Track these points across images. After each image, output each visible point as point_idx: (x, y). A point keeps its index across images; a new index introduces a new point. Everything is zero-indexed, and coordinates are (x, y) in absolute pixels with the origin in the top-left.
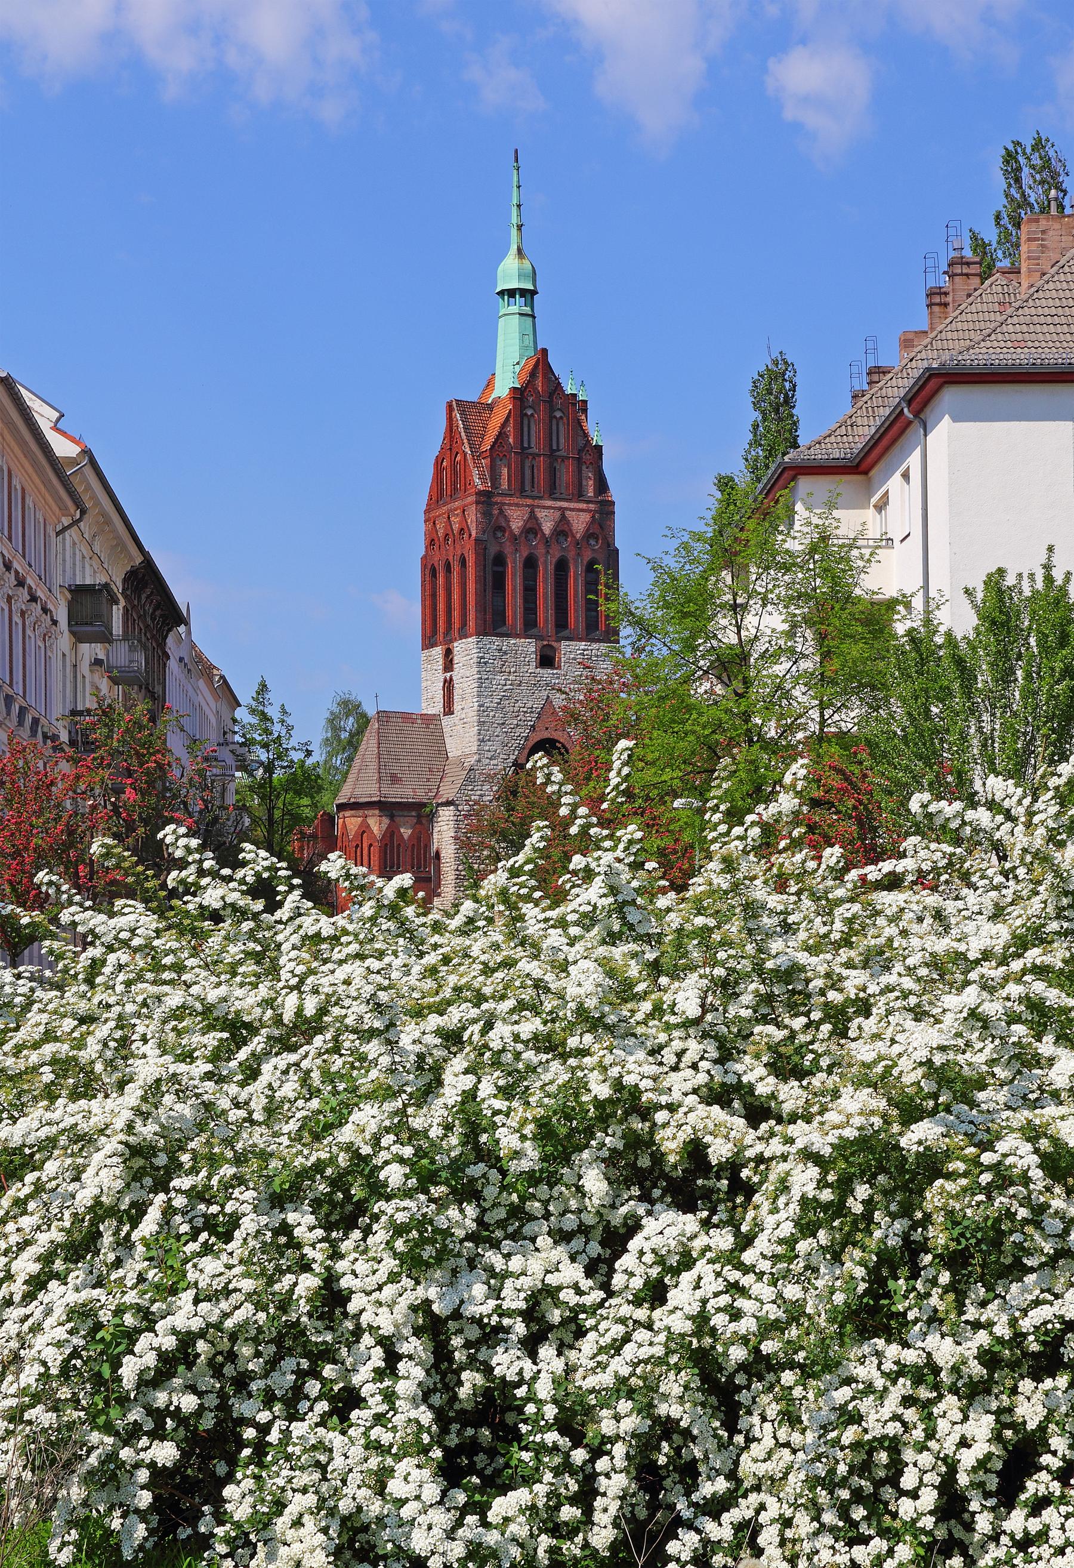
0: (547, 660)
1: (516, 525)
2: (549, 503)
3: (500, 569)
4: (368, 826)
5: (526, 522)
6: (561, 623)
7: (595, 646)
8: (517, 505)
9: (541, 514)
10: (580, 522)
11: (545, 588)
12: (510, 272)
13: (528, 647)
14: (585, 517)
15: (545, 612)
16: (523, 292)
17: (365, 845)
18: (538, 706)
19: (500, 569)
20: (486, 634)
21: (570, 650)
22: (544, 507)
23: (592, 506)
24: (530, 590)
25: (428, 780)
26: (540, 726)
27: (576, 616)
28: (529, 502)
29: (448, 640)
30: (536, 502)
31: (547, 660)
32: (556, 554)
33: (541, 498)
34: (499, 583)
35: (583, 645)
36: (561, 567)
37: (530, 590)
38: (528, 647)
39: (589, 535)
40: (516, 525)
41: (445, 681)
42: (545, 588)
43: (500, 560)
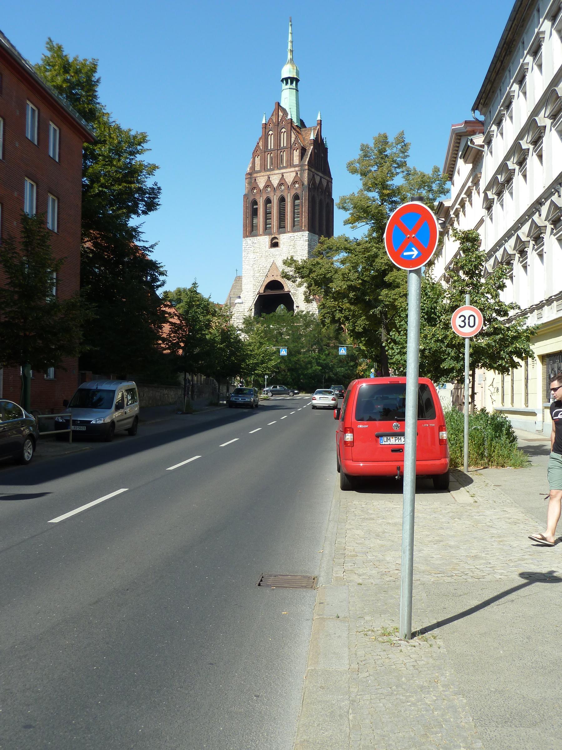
0: (275, 245)
1: (261, 185)
7: (296, 234)
8: (263, 176)
12: (287, 71)
13: (265, 240)
16: (292, 79)
20: (247, 237)
23: (297, 169)
24: (267, 214)
26: (269, 274)
32: (279, 194)
33: (273, 170)
34: (255, 213)
36: (282, 200)
37: (267, 214)
38: (265, 240)
39: (294, 182)
43: (255, 203)
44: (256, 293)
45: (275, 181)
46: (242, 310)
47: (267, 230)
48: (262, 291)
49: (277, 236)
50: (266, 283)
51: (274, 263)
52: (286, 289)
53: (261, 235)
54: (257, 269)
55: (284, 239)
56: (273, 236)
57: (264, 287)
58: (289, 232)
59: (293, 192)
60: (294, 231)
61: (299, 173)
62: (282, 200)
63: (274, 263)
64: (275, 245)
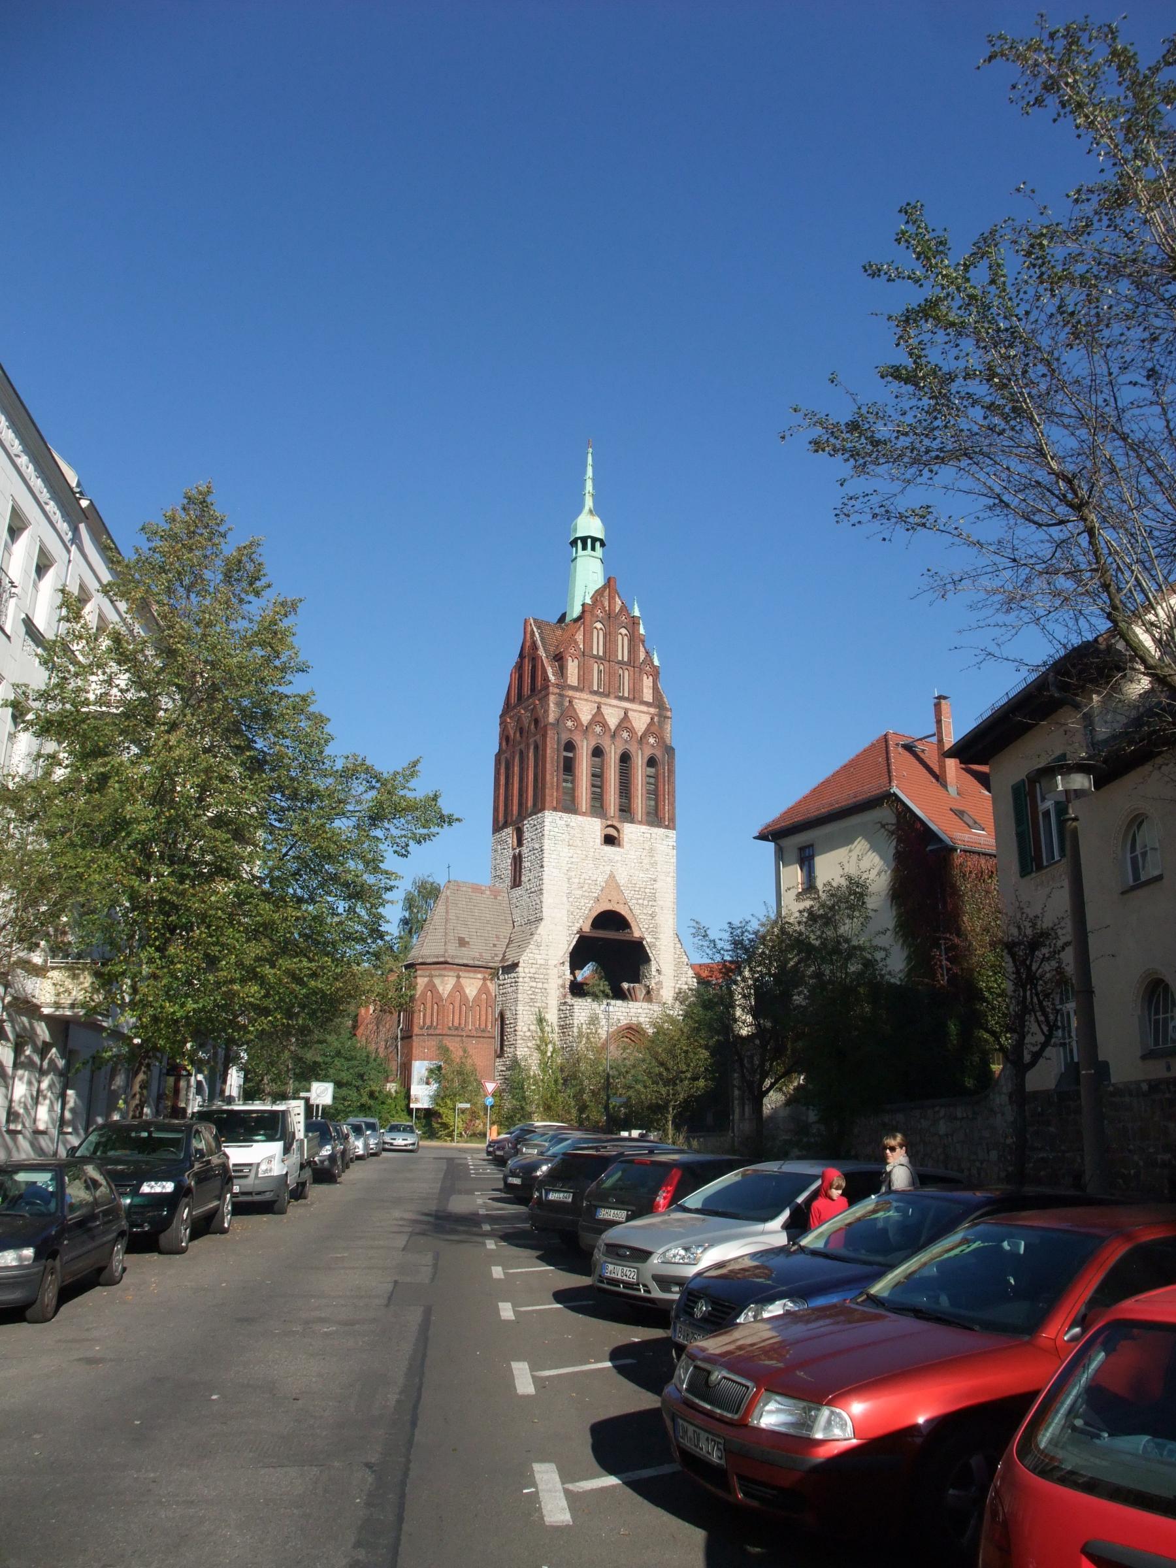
2: (615, 702)
3: (570, 755)
4: (434, 986)
5: (594, 716)
6: (626, 811)
9: (606, 710)
10: (641, 720)
13: (594, 827)
14: (647, 719)
18: (601, 880)
19: (570, 755)
21: (631, 832)
25: (495, 945)
27: (639, 803)
28: (597, 699)
30: (604, 700)
36: (625, 758)
37: (598, 777)
38: (594, 827)
40: (585, 716)
41: (514, 857)
44: (575, 929)
45: (612, 718)
46: (542, 962)
47: (598, 807)
48: (587, 928)
51: (612, 877)
52: (637, 934)
53: (584, 814)
54: (577, 880)
55: (631, 832)
56: (609, 823)
58: (640, 823)
59: (648, 752)
60: (651, 824)
61: (656, 719)
62: (625, 758)
63: (612, 877)
64: (610, 840)
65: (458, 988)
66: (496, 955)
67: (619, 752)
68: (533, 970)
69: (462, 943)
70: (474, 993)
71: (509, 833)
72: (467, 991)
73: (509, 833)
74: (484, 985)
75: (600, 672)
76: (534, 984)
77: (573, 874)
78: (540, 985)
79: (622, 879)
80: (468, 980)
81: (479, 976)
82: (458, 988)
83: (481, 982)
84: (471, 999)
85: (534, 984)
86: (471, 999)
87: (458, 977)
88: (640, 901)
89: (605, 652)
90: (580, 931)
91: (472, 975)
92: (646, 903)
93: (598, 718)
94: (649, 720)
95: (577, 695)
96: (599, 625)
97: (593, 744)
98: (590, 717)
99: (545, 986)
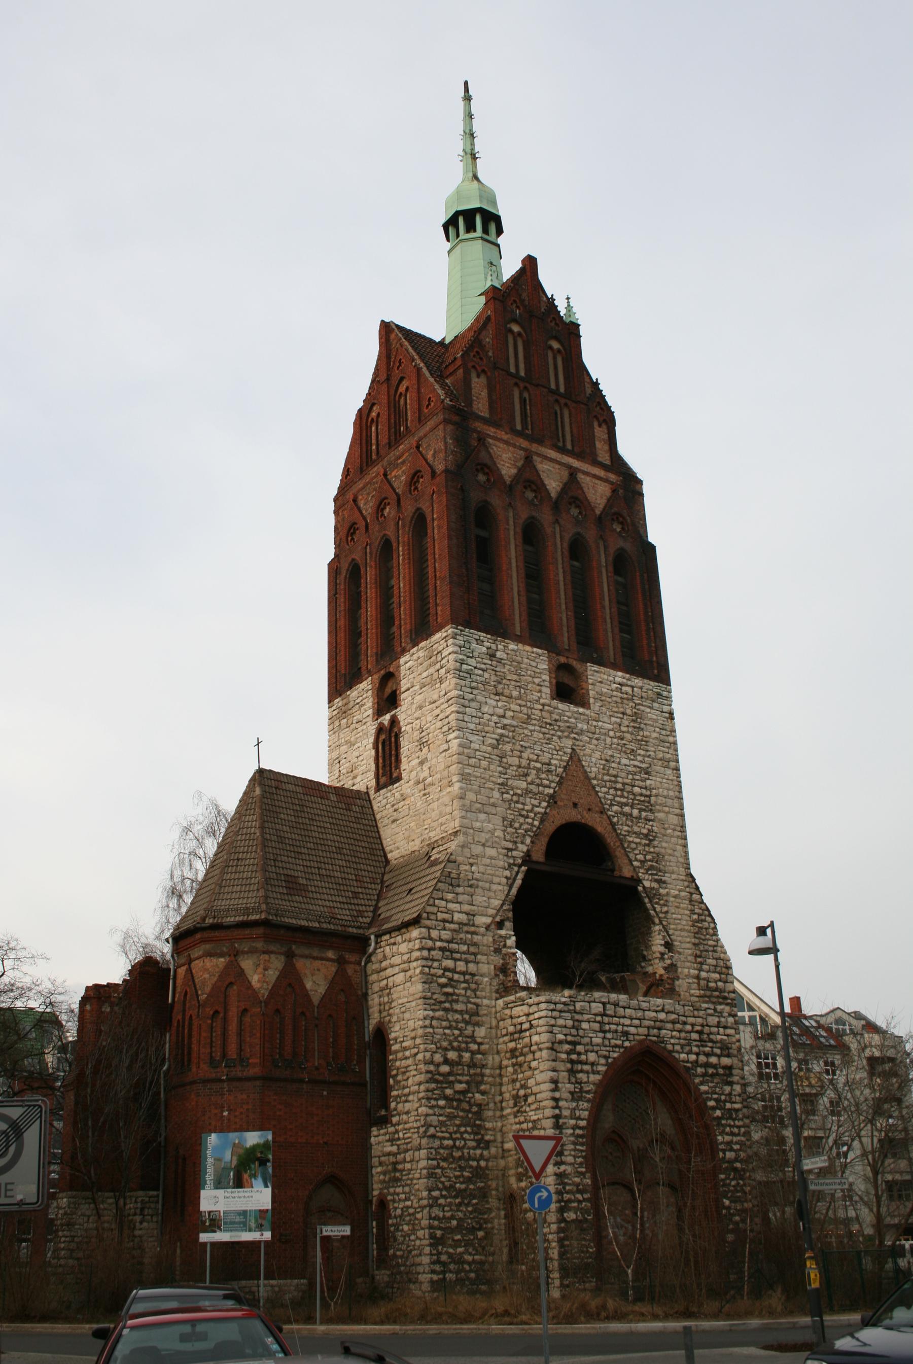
0: (567, 690)
2: (553, 454)
3: (483, 534)
7: (638, 682)
11: (558, 573)
13: (536, 664)
15: (562, 615)
17: (233, 1012)
18: (558, 762)
20: (468, 624)
22: (546, 458)
25: (356, 895)
27: (608, 632)
29: (390, 650)
30: (534, 447)
31: (567, 690)
35: (619, 676)
37: (534, 575)
41: (380, 730)
42: (558, 573)
46: (463, 918)
49: (574, 663)
50: (550, 828)
51: (574, 757)
52: (627, 872)
54: (515, 761)
56: (563, 660)
57: (543, 842)
63: (574, 757)
65: (290, 980)
66: (361, 914)
67: (567, 537)
68: (446, 935)
69: (293, 886)
70: (322, 990)
71: (364, 693)
72: (309, 985)
73: (364, 693)
74: (341, 972)
75: (523, 402)
76: (449, 963)
77: (508, 747)
78: (461, 966)
79: (593, 762)
80: (308, 962)
81: (330, 954)
82: (290, 980)
83: (333, 968)
84: (316, 1000)
85: (449, 963)
86: (316, 1000)
87: (290, 956)
88: (627, 809)
89: (528, 370)
90: (527, 859)
91: (316, 952)
92: (635, 812)
93: (529, 479)
94: (608, 493)
95: (491, 431)
96: (516, 328)
97: (524, 515)
98: (514, 471)
99: (472, 967)
